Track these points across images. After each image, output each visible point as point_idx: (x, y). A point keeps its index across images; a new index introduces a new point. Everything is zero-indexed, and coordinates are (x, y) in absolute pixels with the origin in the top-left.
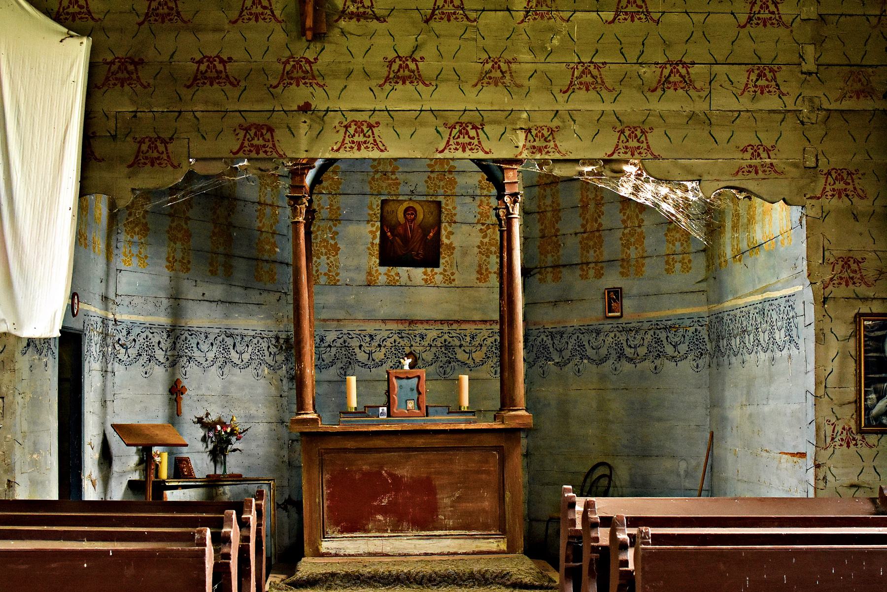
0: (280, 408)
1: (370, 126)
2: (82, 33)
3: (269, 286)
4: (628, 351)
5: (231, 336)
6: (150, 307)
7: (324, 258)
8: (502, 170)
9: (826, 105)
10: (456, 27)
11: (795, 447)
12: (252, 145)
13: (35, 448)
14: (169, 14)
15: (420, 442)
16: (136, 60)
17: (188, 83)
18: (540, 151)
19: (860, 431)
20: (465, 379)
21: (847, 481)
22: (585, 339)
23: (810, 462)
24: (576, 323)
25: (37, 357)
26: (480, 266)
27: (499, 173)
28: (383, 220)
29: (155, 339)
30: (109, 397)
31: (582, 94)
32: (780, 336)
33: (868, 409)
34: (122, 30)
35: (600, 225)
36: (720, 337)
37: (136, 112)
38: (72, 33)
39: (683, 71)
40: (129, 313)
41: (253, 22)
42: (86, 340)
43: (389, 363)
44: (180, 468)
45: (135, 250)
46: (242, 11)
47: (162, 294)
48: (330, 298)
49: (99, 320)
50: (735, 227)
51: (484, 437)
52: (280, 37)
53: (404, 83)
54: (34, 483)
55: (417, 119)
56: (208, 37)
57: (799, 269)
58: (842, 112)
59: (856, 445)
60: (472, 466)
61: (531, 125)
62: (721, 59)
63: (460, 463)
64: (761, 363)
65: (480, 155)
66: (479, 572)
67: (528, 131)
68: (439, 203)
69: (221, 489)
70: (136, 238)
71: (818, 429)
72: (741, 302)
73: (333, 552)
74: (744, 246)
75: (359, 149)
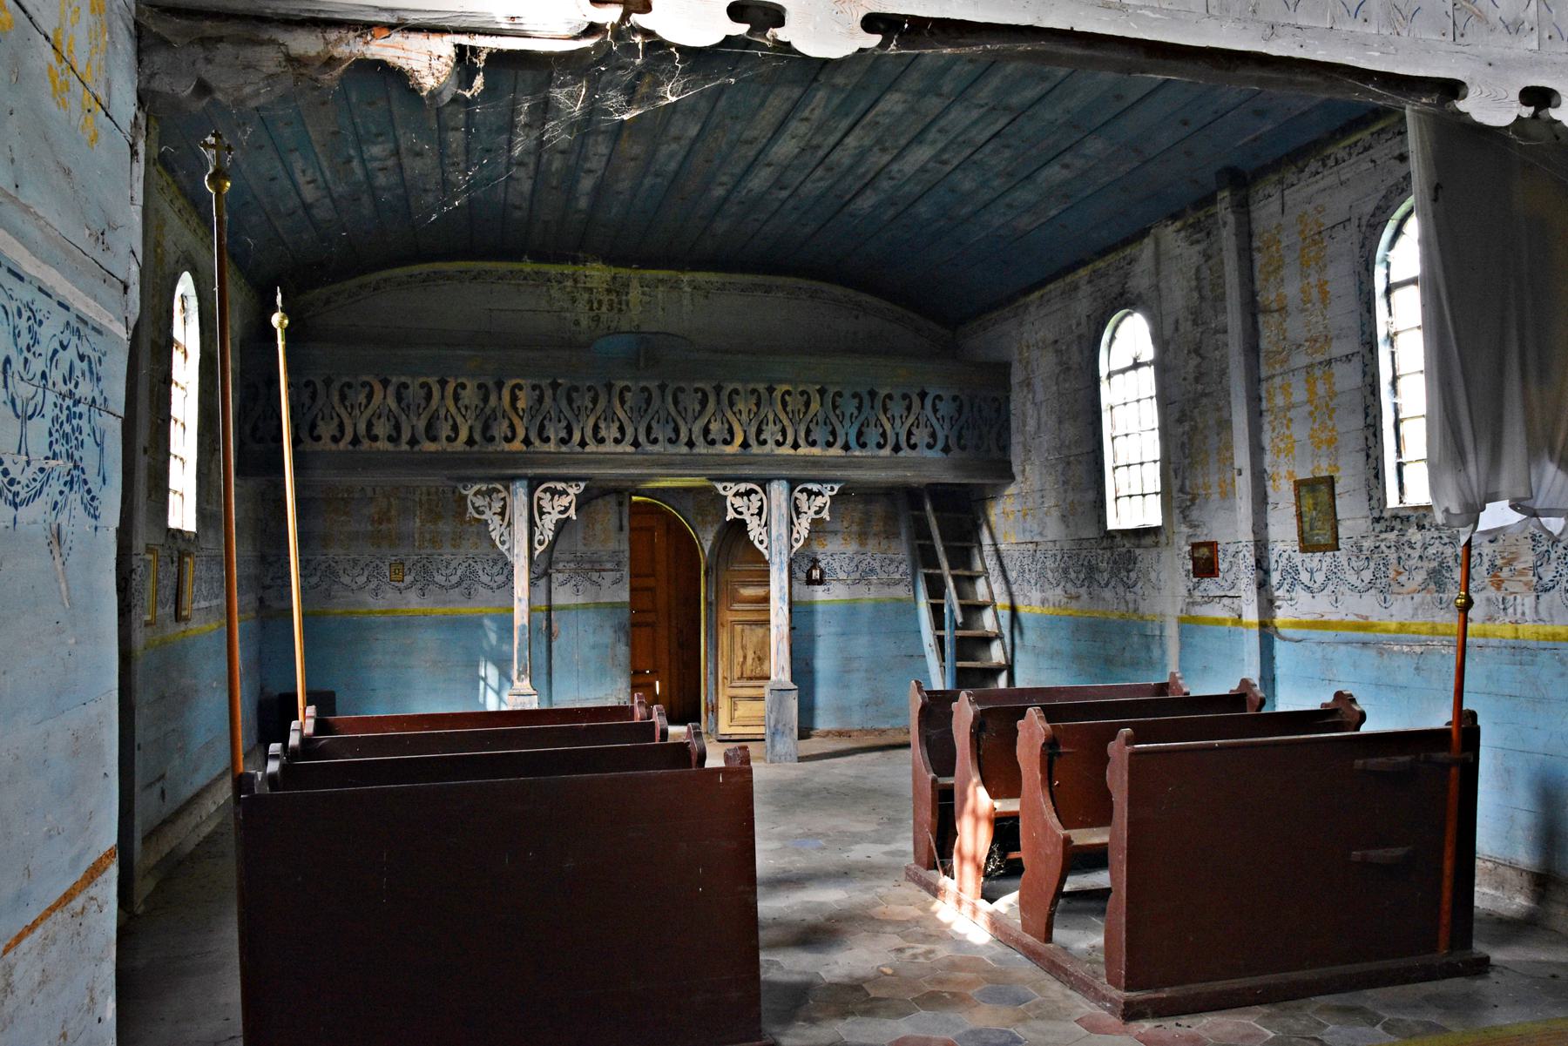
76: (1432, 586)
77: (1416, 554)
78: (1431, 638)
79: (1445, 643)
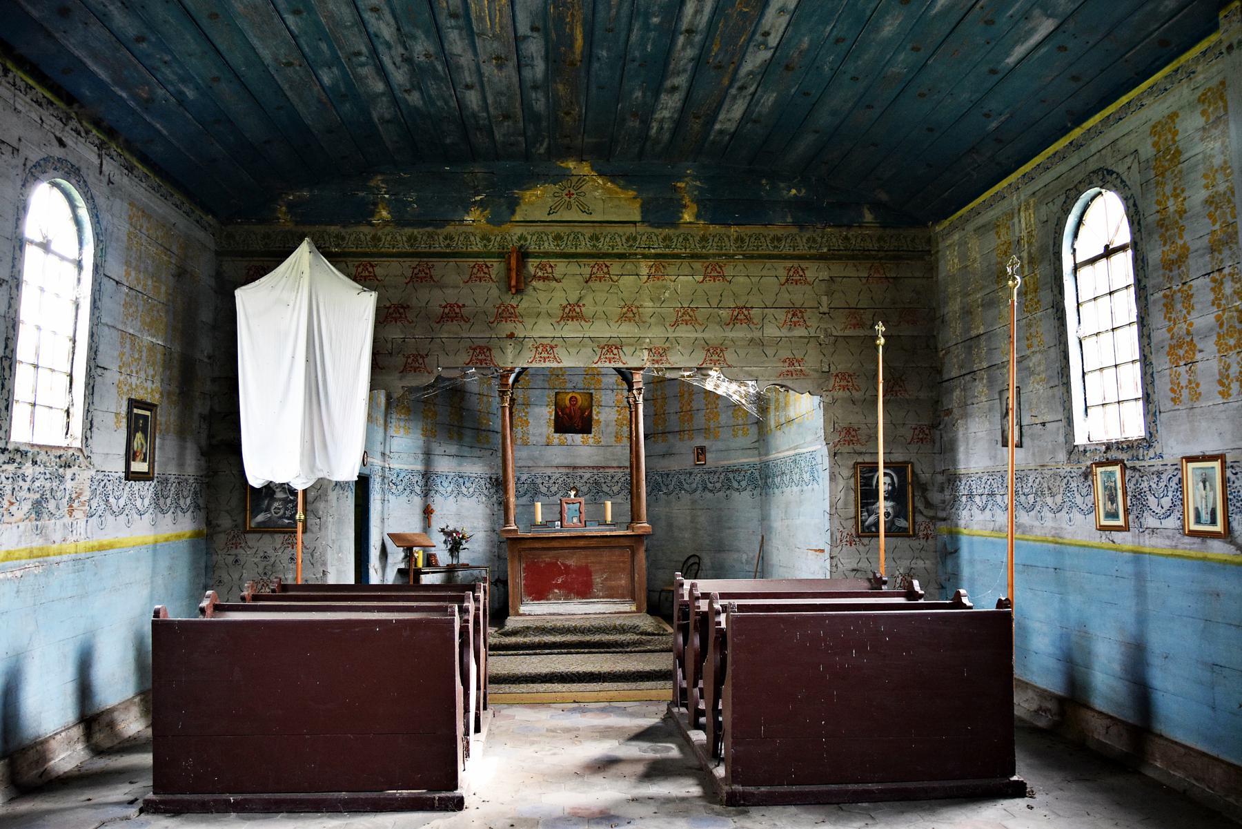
0: (493, 522)
1: (552, 348)
2: (371, 288)
3: (486, 446)
4: (710, 486)
5: (462, 477)
6: (411, 460)
7: (520, 428)
8: (632, 374)
9: (835, 334)
10: (604, 286)
11: (817, 546)
12: (478, 359)
13: (340, 550)
15: (582, 543)
18: (657, 362)
19: (858, 536)
20: (609, 504)
21: (850, 567)
22: (682, 478)
23: (827, 555)
24: (676, 468)
25: (341, 492)
26: (617, 433)
27: (629, 376)
28: (556, 404)
29: (414, 480)
30: (386, 517)
31: (683, 327)
32: (806, 477)
33: (863, 522)
35: (692, 407)
36: (767, 477)
39: (746, 313)
40: (398, 463)
41: (478, 282)
42: (372, 481)
43: (561, 494)
44: (430, 561)
45: (402, 424)
46: (471, 275)
47: (419, 451)
48: (524, 453)
50: (777, 409)
51: (622, 540)
52: (495, 292)
53: (572, 320)
54: (339, 572)
55: (581, 343)
56: (449, 291)
57: (818, 435)
58: (845, 337)
59: (856, 544)
60: (614, 558)
61: (652, 346)
62: (769, 304)
63: (606, 556)
64: (794, 493)
65: (620, 365)
66: (620, 625)
67: (650, 350)
68: (591, 394)
69: (456, 574)
70: (403, 417)
71: (832, 535)
72: (781, 455)
73: (527, 613)
74: (783, 420)
75: (545, 362)
76: (33, 515)
77: (25, 486)
78: (28, 561)
79: (37, 564)
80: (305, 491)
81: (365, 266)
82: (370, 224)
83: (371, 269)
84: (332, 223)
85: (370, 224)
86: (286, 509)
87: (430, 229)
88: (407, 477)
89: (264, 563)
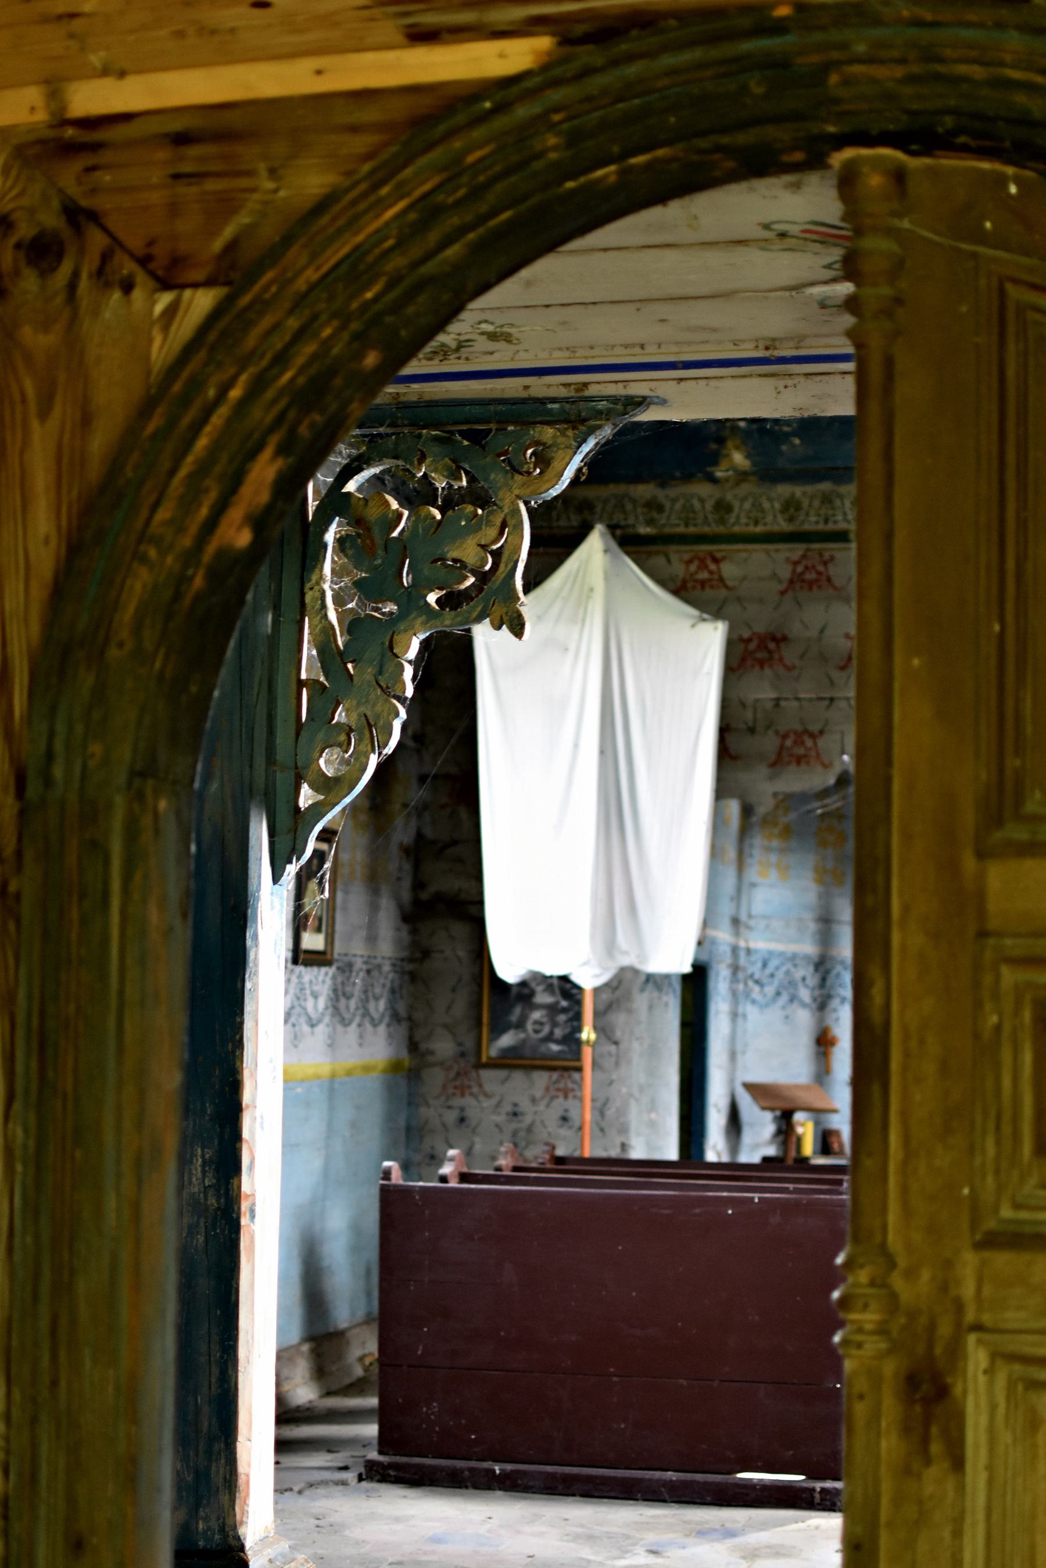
2: (717, 614)
13: (653, 1106)
14: (817, 580)
16: (779, 635)
17: (843, 664)
25: (656, 994)
29: (799, 974)
30: (739, 1048)
34: (761, 601)
37: (778, 700)
38: (705, 616)
45: (773, 858)
49: (728, 949)
80: (597, 991)
81: (702, 561)
82: (713, 480)
83: (713, 567)
84: (637, 479)
85: (713, 480)
86: (555, 1024)
87: (826, 486)
88: (784, 969)
89: (514, 1125)
